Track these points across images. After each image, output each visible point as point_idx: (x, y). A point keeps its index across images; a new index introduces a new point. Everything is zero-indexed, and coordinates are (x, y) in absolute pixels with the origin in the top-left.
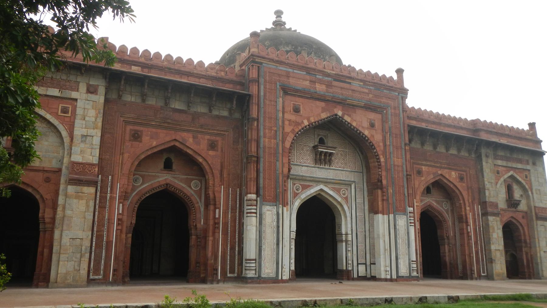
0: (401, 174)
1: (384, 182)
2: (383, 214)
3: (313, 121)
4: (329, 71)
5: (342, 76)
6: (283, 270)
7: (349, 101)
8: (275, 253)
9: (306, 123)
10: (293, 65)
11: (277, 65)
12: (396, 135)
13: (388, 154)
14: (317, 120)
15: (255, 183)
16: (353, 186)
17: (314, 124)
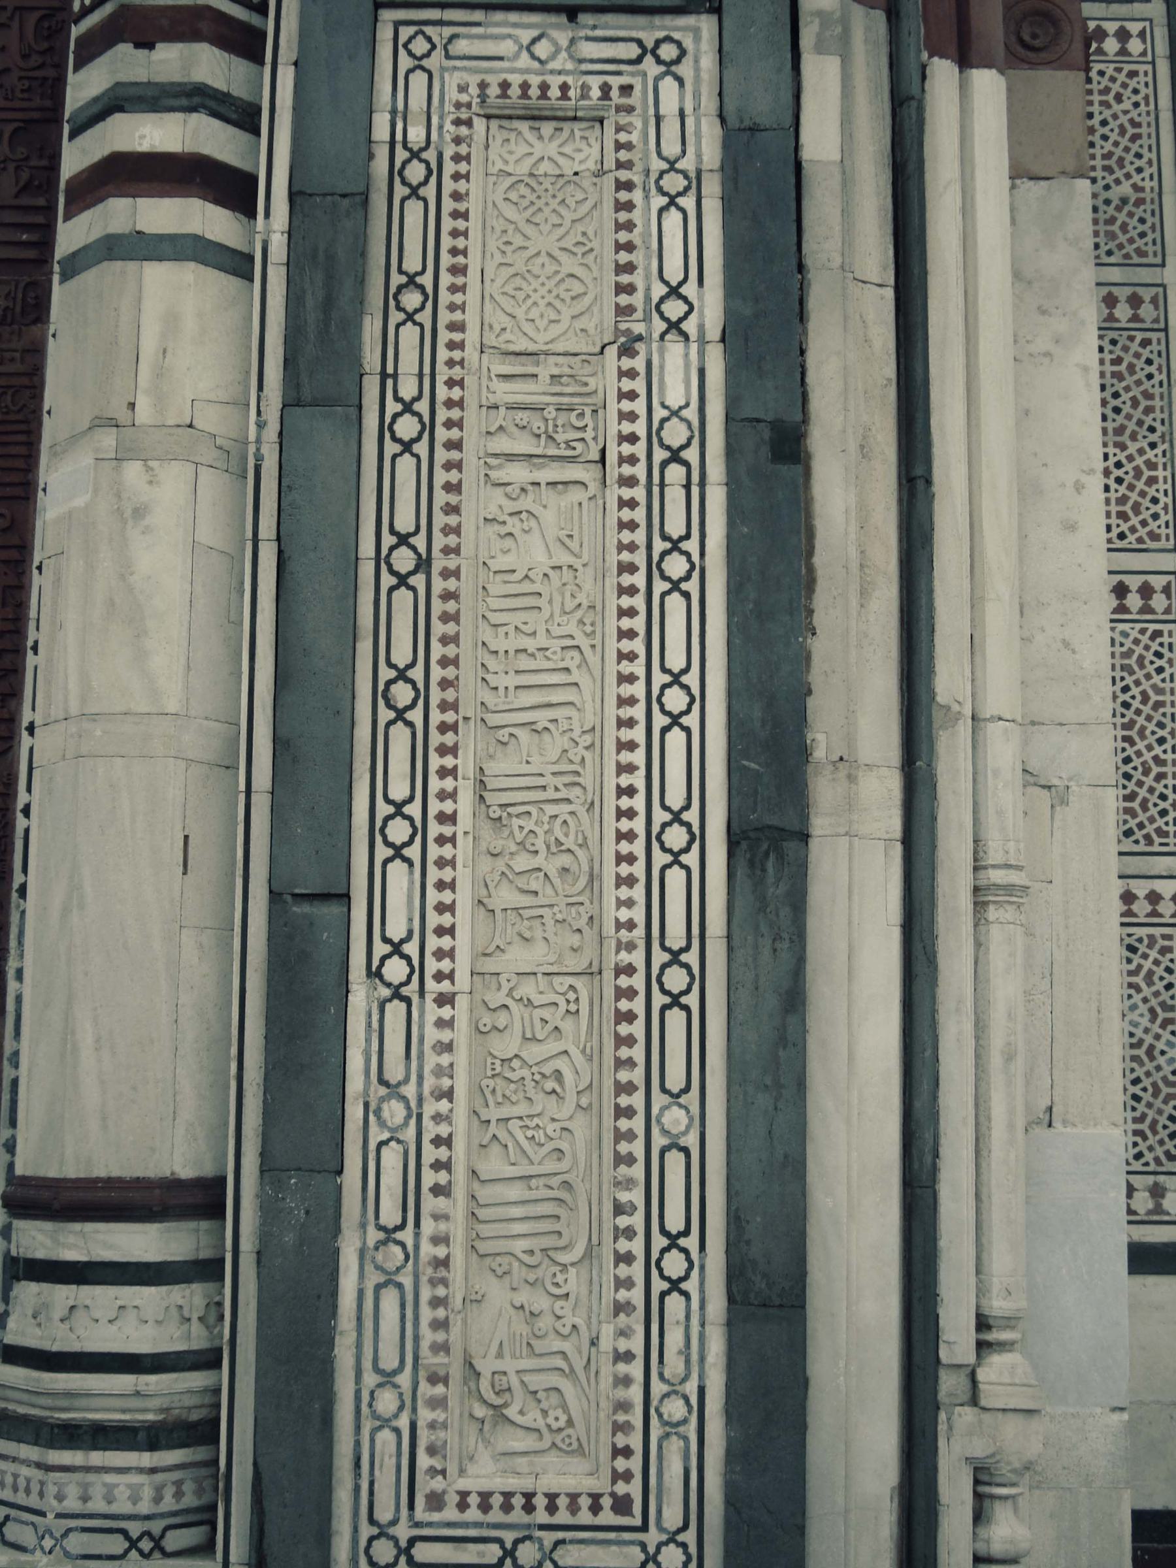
8: (700, 1047)
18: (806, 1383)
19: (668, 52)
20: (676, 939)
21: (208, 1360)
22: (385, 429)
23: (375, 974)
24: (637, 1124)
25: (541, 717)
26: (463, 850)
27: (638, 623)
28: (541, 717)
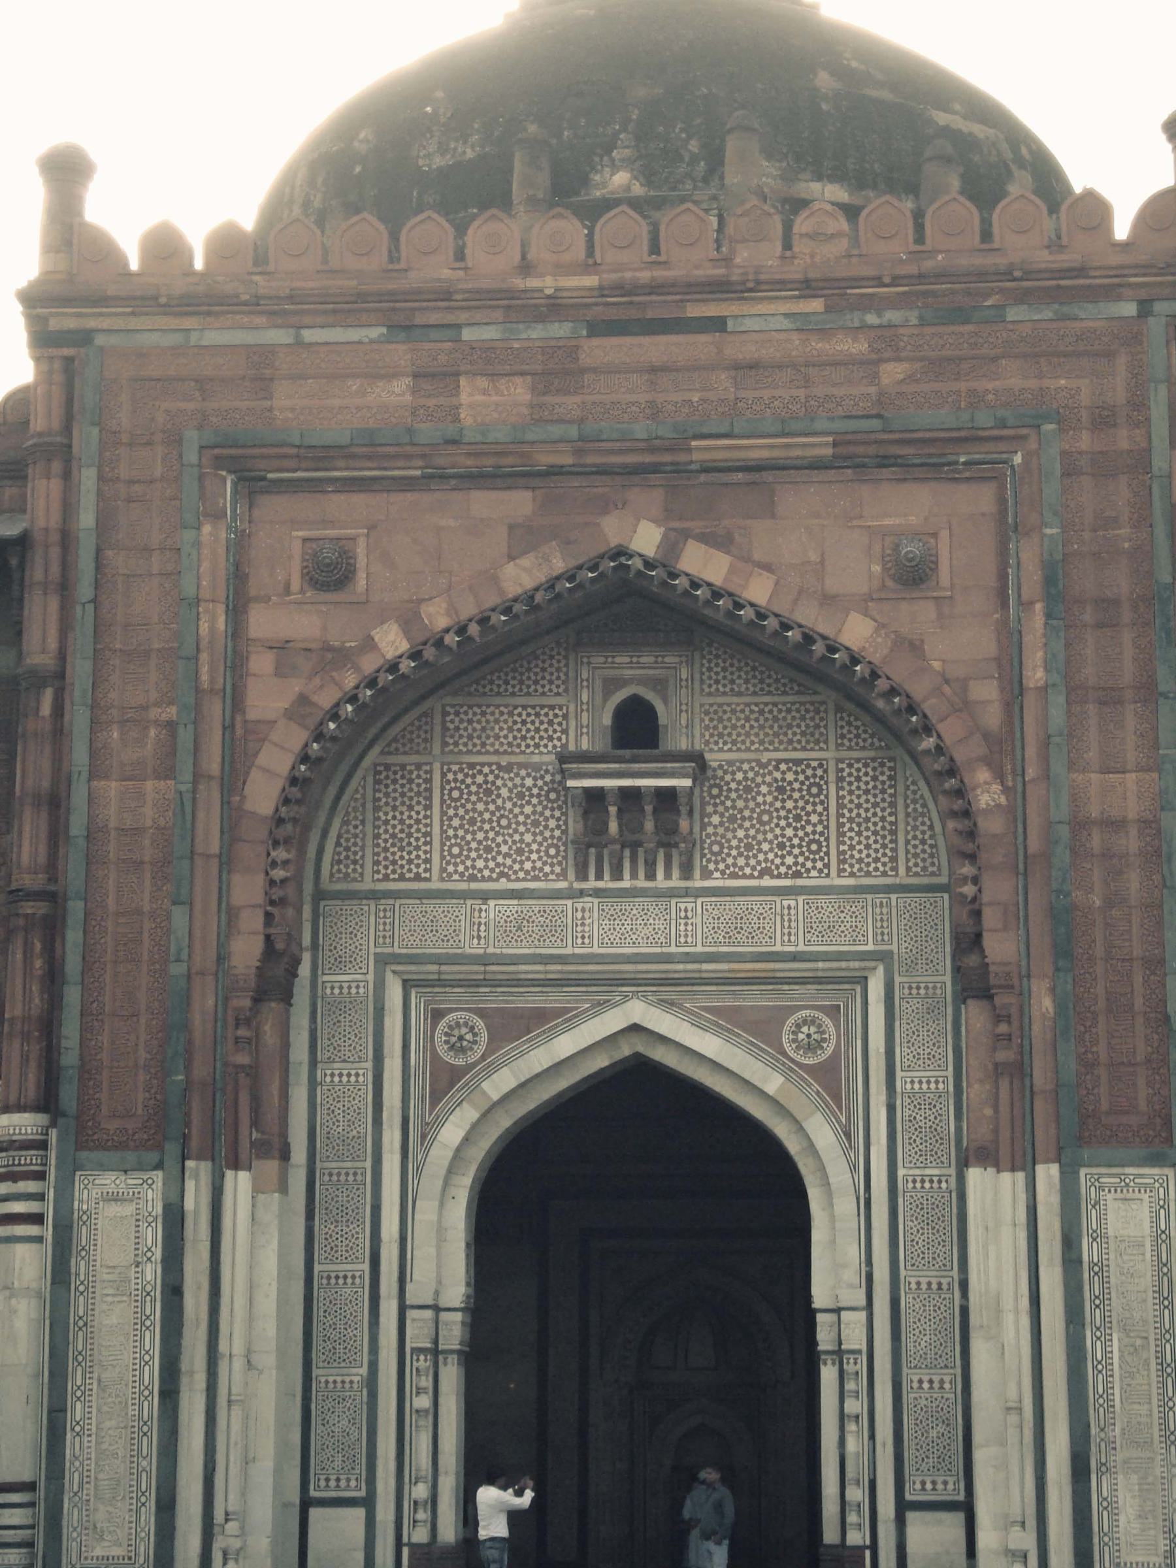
0: (1134, 883)
1: (1000, 947)
2: (998, 1172)
3: (442, 622)
4: (548, 284)
5: (654, 288)
6: (218, 1544)
7: (702, 450)
8: (151, 1445)
9: (392, 642)
10: (291, 298)
11: (188, 323)
12: (1107, 605)
13: (1031, 752)
14: (468, 609)
15: (35, 1050)
16: (876, 987)
17: (452, 639)
18: (174, 1528)
19: (150, 1181)
20: (146, 1418)
21: (32, 1527)
22: (76, 1288)
23: (73, 1429)
24: (135, 1465)
25: (115, 1363)
26: (94, 1398)
27: (138, 1338)
28: (115, 1363)
